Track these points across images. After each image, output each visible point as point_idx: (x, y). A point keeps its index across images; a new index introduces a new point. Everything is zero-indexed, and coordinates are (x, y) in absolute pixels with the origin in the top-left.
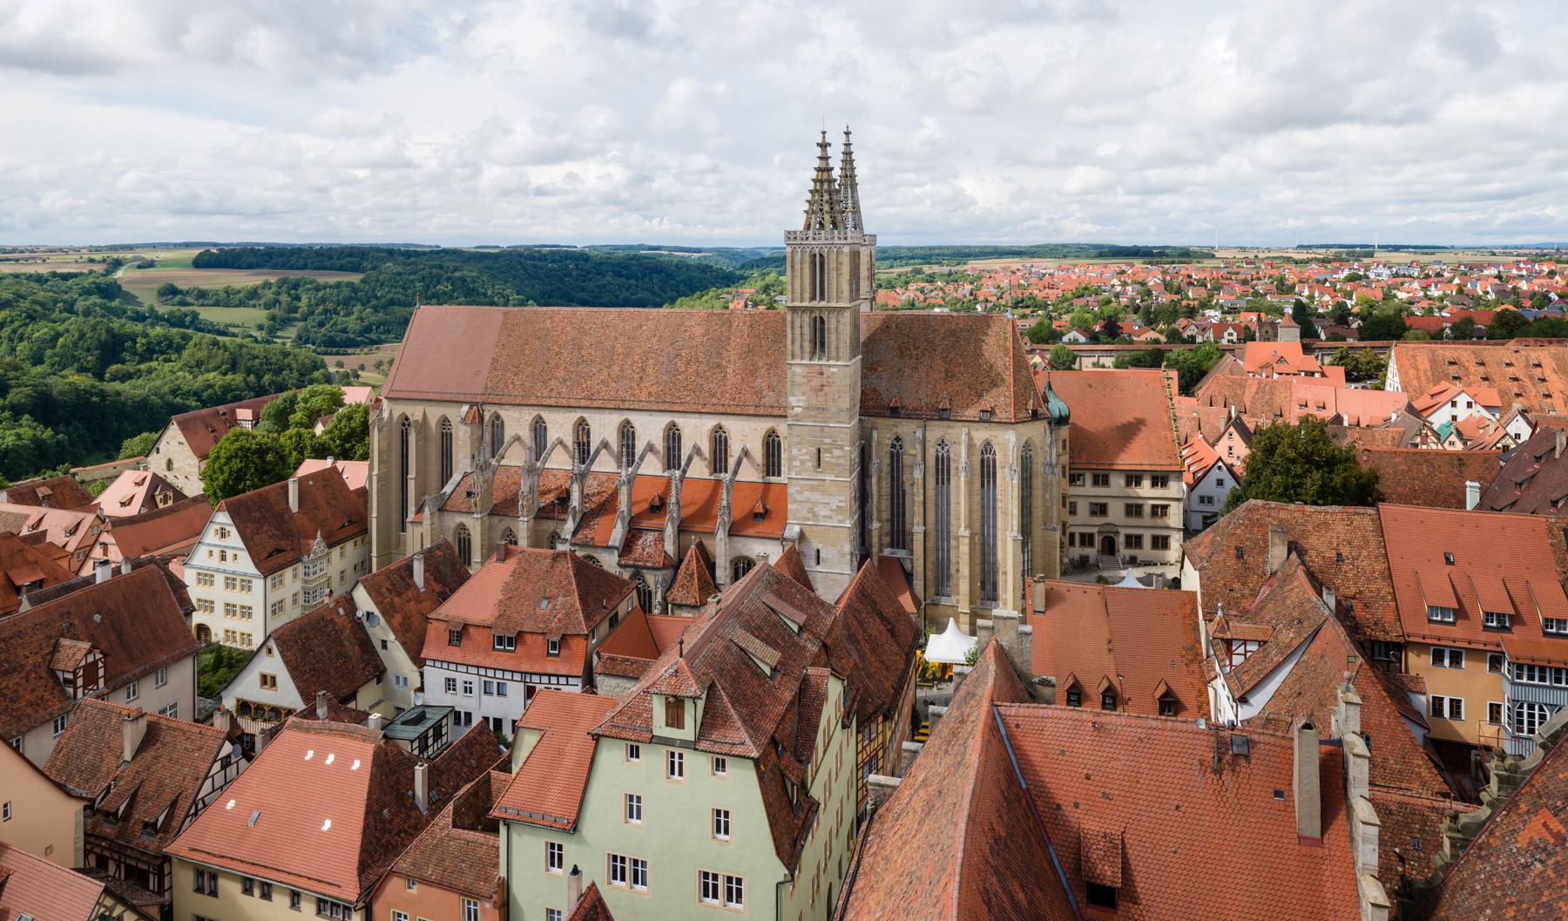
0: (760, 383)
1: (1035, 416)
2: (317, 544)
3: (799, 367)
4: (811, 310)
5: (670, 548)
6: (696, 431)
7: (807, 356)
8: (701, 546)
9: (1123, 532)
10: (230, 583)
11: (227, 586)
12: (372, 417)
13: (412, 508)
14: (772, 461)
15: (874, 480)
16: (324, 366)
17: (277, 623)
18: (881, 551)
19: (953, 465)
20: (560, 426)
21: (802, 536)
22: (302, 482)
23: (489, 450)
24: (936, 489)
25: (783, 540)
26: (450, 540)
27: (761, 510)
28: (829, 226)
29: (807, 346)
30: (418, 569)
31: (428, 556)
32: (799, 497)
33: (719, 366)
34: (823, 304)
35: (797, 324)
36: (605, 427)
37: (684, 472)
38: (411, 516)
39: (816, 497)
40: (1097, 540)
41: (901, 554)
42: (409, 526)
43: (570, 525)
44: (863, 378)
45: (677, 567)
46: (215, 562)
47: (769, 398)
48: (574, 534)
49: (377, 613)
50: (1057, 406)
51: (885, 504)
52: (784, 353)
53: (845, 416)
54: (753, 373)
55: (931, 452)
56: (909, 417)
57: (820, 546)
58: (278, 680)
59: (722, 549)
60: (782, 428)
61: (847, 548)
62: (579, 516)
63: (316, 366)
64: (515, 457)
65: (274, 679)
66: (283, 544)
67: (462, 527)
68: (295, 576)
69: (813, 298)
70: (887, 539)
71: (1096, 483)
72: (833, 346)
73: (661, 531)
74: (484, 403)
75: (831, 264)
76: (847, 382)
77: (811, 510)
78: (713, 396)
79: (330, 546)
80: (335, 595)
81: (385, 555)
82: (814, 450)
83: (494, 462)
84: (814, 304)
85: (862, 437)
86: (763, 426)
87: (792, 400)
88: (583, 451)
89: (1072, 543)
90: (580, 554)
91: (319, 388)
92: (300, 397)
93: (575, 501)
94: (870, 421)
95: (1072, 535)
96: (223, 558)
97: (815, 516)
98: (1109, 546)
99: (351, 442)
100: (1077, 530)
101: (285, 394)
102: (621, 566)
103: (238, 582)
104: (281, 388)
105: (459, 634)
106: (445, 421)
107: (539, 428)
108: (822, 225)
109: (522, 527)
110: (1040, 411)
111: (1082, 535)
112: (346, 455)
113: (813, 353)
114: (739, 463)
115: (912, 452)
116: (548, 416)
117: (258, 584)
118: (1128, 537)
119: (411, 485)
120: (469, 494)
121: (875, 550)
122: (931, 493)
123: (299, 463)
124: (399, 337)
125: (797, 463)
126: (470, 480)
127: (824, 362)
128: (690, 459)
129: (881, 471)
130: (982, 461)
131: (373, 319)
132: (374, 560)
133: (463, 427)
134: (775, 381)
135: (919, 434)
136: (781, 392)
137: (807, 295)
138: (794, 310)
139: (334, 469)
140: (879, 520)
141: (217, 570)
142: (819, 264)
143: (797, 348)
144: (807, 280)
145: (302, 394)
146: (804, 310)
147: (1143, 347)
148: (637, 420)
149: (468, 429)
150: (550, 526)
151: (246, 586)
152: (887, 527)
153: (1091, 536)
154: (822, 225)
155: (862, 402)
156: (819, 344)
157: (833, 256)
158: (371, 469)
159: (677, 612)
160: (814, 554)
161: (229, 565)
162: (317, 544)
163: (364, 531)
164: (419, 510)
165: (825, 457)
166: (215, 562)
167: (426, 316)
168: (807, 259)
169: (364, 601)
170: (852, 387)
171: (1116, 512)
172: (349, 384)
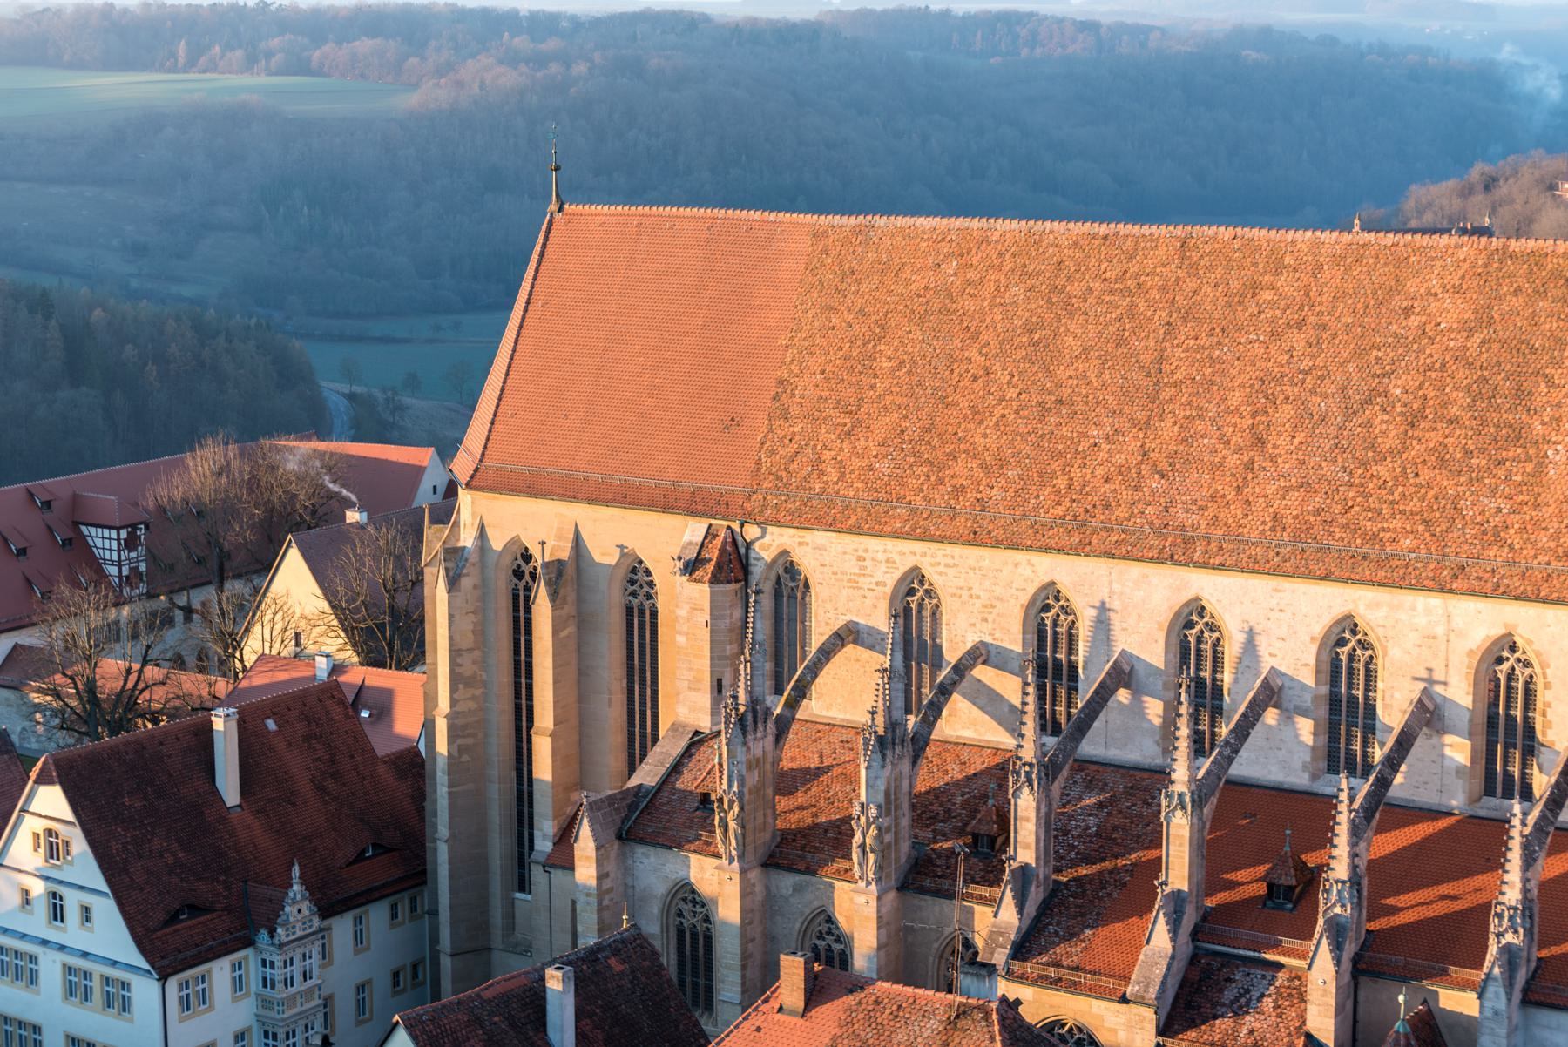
2: (298, 907)
10: (76, 985)
11: (70, 990)
26: (652, 928)
33: (1518, 435)
37: (1383, 783)
46: (38, 923)
62: (1036, 895)
64: (847, 695)
67: (687, 897)
68: (238, 984)
78: (1497, 538)
93: (1026, 846)
96: (57, 913)
103: (96, 984)
109: (858, 906)
117: (145, 991)
141: (45, 943)
150: (940, 914)
151: (118, 1000)
161: (72, 933)
162: (298, 907)
163: (409, 872)
166: (38, 923)
167: (590, 240)
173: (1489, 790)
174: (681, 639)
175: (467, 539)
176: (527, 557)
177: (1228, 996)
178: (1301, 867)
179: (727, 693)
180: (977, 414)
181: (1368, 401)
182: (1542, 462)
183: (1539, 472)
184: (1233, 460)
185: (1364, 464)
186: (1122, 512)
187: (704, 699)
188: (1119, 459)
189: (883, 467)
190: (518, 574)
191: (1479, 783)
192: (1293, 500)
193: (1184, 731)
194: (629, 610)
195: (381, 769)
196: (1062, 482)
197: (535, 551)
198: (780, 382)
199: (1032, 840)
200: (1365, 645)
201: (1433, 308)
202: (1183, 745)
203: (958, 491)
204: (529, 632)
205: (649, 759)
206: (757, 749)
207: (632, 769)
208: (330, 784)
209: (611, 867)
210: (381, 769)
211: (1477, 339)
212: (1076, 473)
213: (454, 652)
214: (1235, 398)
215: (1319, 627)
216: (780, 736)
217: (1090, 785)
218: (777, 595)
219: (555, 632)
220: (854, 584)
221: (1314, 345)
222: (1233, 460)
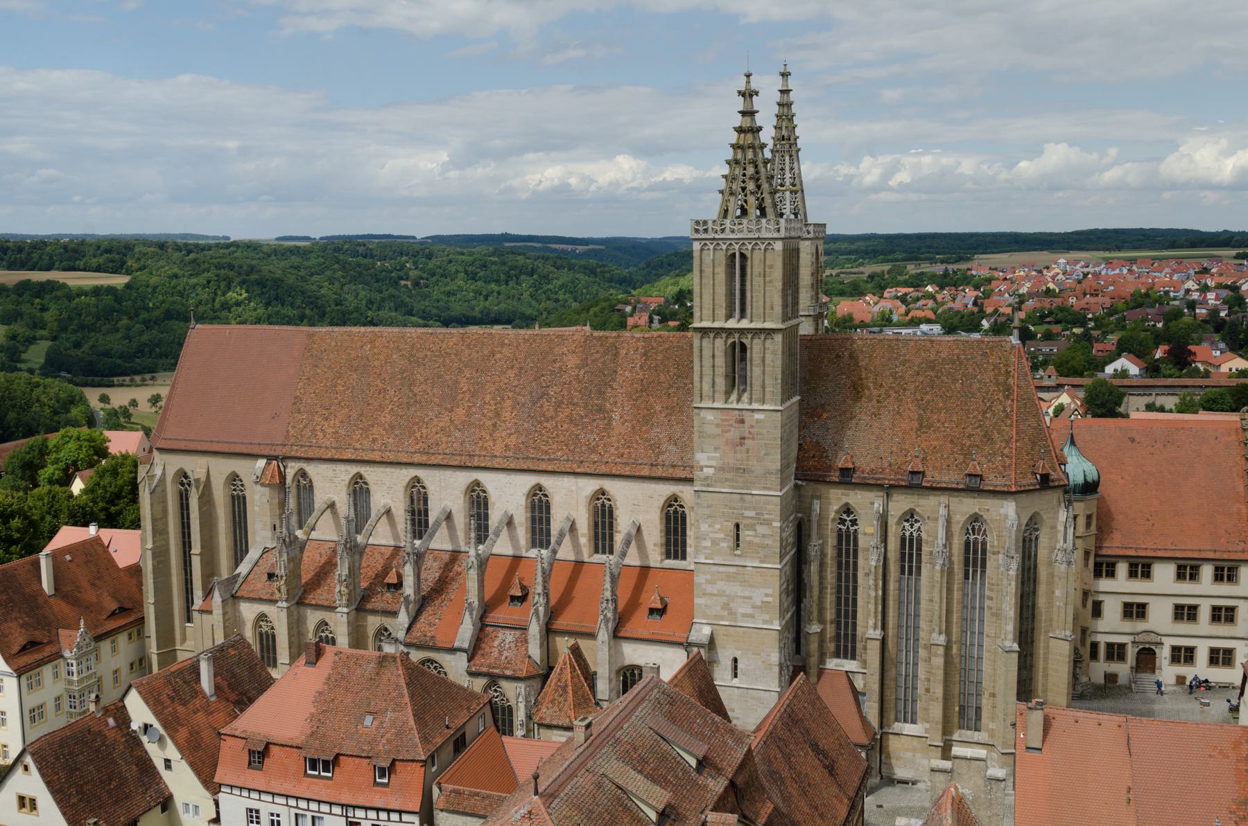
0: (659, 433)
1: (1045, 482)
3: (711, 409)
4: (730, 332)
5: (535, 651)
6: (570, 499)
7: (720, 396)
8: (576, 651)
9: (1168, 642)
12: (142, 471)
13: (198, 593)
14: (675, 541)
15: (814, 568)
16: (83, 400)
17: (36, 733)
18: (822, 661)
19: (925, 549)
20: (388, 489)
21: (711, 644)
22: (56, 556)
23: (294, 519)
24: (900, 581)
25: (687, 645)
27: (659, 606)
28: (754, 212)
29: (721, 382)
30: (205, 670)
31: (219, 656)
32: (709, 589)
33: (601, 409)
34: (745, 324)
35: (707, 353)
36: (448, 492)
37: (555, 552)
38: (198, 602)
39: (734, 588)
40: (1131, 653)
41: (850, 665)
42: (196, 615)
43: (403, 618)
44: (802, 427)
45: (545, 678)
47: (671, 453)
48: (409, 629)
49: (157, 725)
50: (1077, 468)
51: (830, 599)
52: (690, 392)
53: (775, 480)
54: (647, 419)
55: (893, 530)
56: (864, 485)
57: (738, 654)
58: (39, 803)
59: (599, 654)
60: (686, 493)
61: (775, 657)
63: (72, 401)
65: (33, 801)
66: (39, 635)
69: (729, 316)
70: (831, 647)
71: (1132, 574)
72: (757, 383)
73: (524, 629)
74: (285, 458)
75: (755, 267)
76: (778, 433)
77: (726, 607)
78: (593, 450)
79: (98, 638)
80: (105, 701)
81: (168, 656)
82: (731, 526)
83: (299, 534)
84: (732, 324)
85: (798, 509)
86: (664, 490)
87: (701, 458)
88: (419, 521)
89: (1094, 655)
90: (416, 656)
91: (74, 432)
92: (51, 444)
93: (409, 589)
94: (809, 489)
95: (1095, 646)
97: (732, 614)
98: (1146, 659)
99: (115, 506)
100: (1102, 639)
101: (31, 440)
102: (471, 674)
104: (30, 432)
105: (259, 755)
106: (234, 478)
107: (359, 491)
108: (744, 212)
110: (1054, 475)
111: (1110, 646)
112: (111, 521)
113: (728, 394)
114: (627, 543)
115: (867, 531)
116: (371, 475)
118: (1176, 649)
119: (196, 562)
120: (271, 576)
121: (814, 660)
122: (892, 586)
123: (53, 532)
124: (172, 367)
125: (708, 543)
126: (272, 558)
127: (744, 405)
128: (561, 535)
129: (823, 555)
130: (967, 543)
131: (145, 337)
132: (155, 659)
133: (258, 487)
134: (678, 429)
135: (878, 505)
136: (686, 446)
137: (722, 312)
138: (704, 331)
139: (97, 540)
140: (821, 621)
142: (738, 265)
143: (706, 387)
144: (721, 290)
145: (54, 439)
146: (718, 332)
147: (1224, 382)
148: (490, 481)
149: (267, 490)
152: (830, 631)
153: (1122, 646)
154: (744, 212)
155: (798, 460)
156: (737, 378)
157: (758, 256)
158: (143, 541)
159: (544, 733)
160: (729, 663)
164: (208, 593)
165: (745, 535)
168: (721, 258)
169: (139, 711)
170: (785, 441)
171: (1160, 617)
172: (117, 427)
173: (597, 551)
174: (257, 509)
175: (158, 471)
176: (186, 477)
177: (496, 643)
178: (523, 588)
179: (278, 530)
180: (381, 408)
181: (542, 397)
182: (611, 419)
183: (609, 424)
184: (489, 423)
185: (540, 422)
186: (444, 446)
187: (268, 533)
188: (441, 424)
189: (342, 432)
190: (182, 484)
191: (592, 549)
192: (513, 439)
193: (473, 535)
194: (233, 497)
195: (122, 574)
196: (418, 435)
197: (190, 474)
198: (296, 398)
199: (412, 584)
200: (546, 496)
201: (565, 358)
202: (473, 541)
203: (374, 440)
204: (188, 509)
205: (245, 560)
206: (292, 554)
207: (237, 566)
208: (97, 582)
209: (229, 609)
210: (122, 574)
211: (582, 371)
212: (424, 431)
213: (154, 520)
214: (488, 398)
215: (526, 490)
216: (302, 548)
217: (435, 559)
218: (298, 486)
219: (200, 508)
220: (331, 481)
221: (519, 375)
222: (489, 423)
